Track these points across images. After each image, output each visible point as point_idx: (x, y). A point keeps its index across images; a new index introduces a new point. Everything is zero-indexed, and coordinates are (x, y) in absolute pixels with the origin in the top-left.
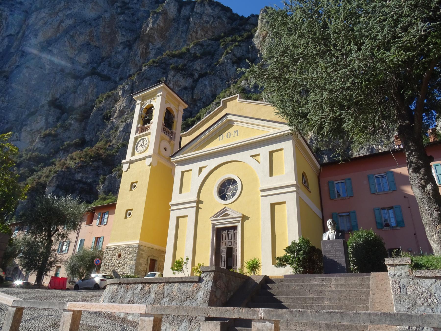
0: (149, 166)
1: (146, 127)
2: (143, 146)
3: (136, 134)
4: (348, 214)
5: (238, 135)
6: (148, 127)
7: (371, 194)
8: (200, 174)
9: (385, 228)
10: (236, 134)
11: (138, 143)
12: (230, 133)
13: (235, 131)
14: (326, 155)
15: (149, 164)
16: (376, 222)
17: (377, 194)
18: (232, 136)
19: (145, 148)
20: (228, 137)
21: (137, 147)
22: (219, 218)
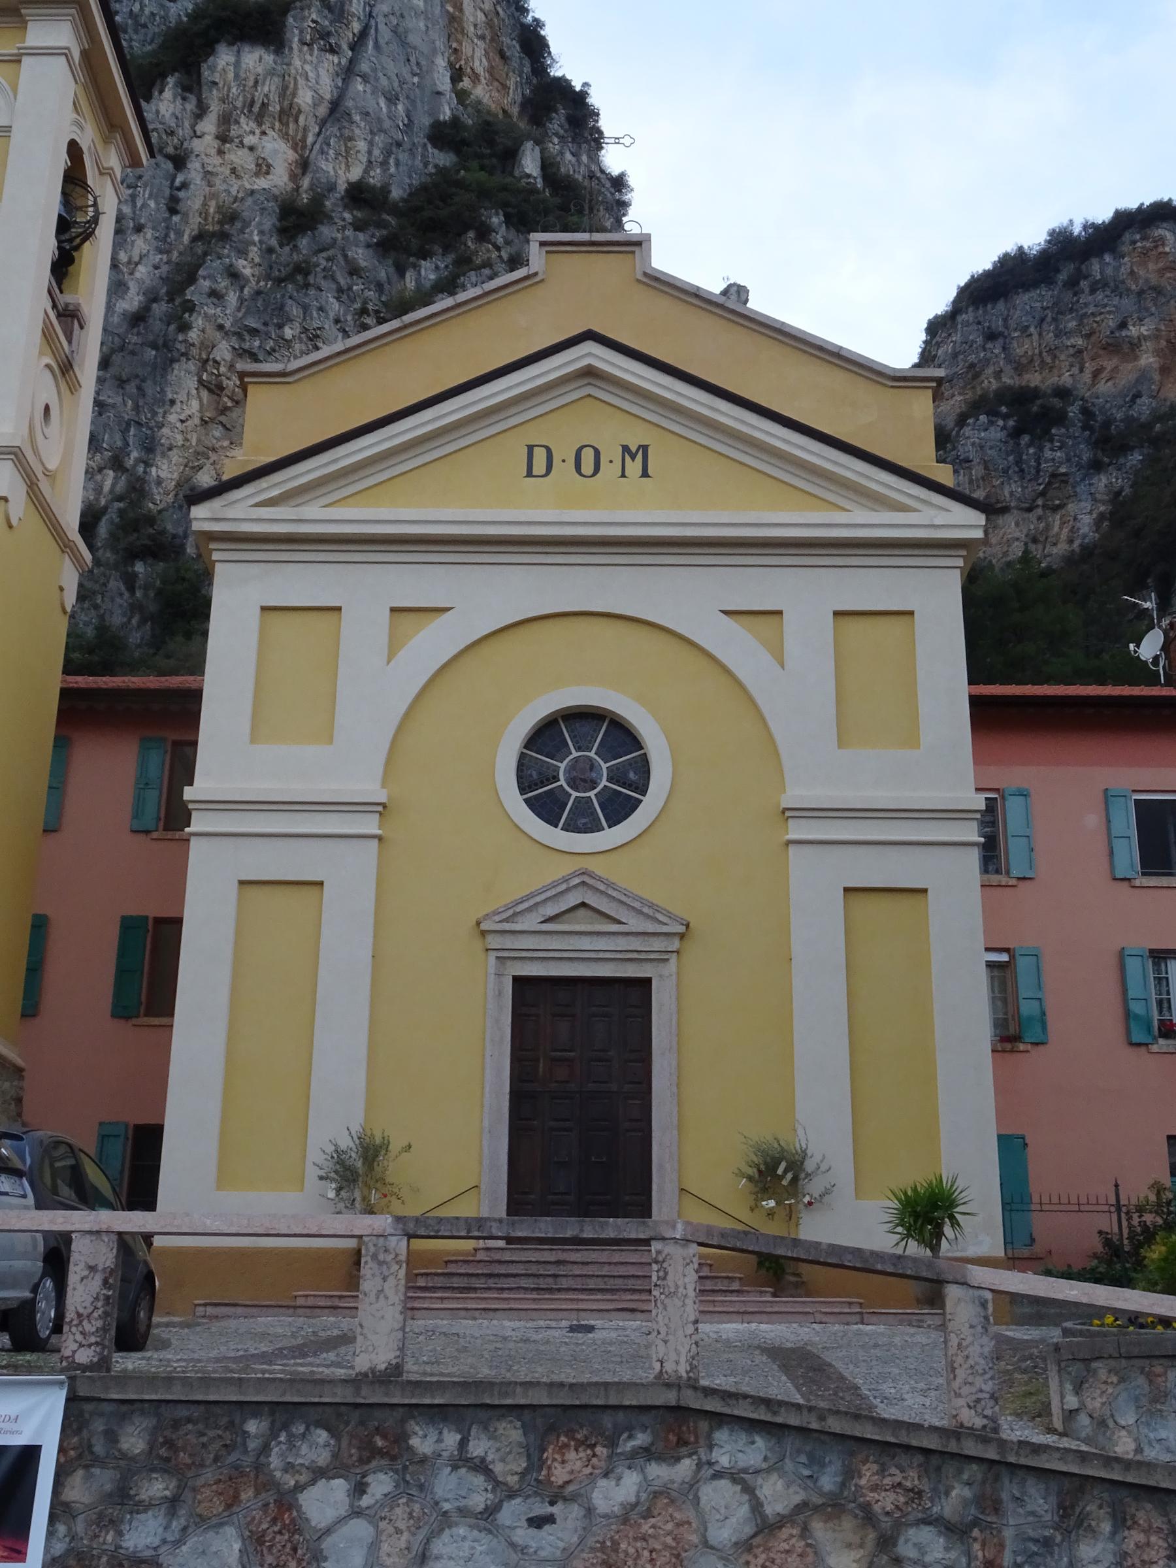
4: (1004, 957)
5: (645, 474)
7: (1115, 879)
8: (402, 654)
9: (1161, 1041)
10: (634, 467)
12: (597, 453)
13: (626, 449)
16: (1128, 1014)
17: (1137, 883)
18: (610, 471)
20: (588, 466)
22: (530, 922)
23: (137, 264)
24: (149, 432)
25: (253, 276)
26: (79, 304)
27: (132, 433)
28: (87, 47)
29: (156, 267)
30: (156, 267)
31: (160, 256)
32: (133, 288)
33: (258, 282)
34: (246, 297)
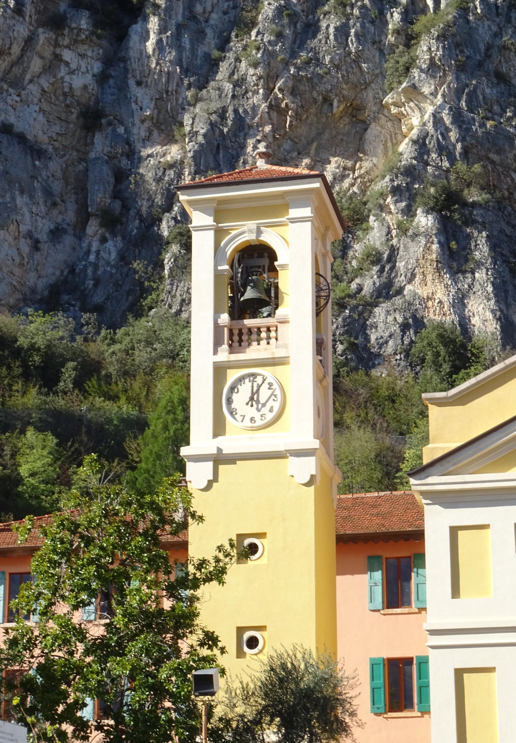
0: (308, 484)
1: (250, 330)
2: (258, 402)
3: (215, 352)
6: (259, 329)
11: (233, 389)
14: (484, 228)
15: (307, 479)
19: (270, 416)
21: (229, 401)
23: (210, 13)
24: (234, 153)
25: (303, 11)
26: (323, 339)
27: (221, 155)
28: (317, 205)
29: (225, 13)
30: (225, 13)
31: (227, 4)
32: (209, 32)
33: (307, 16)
34: (299, 31)
